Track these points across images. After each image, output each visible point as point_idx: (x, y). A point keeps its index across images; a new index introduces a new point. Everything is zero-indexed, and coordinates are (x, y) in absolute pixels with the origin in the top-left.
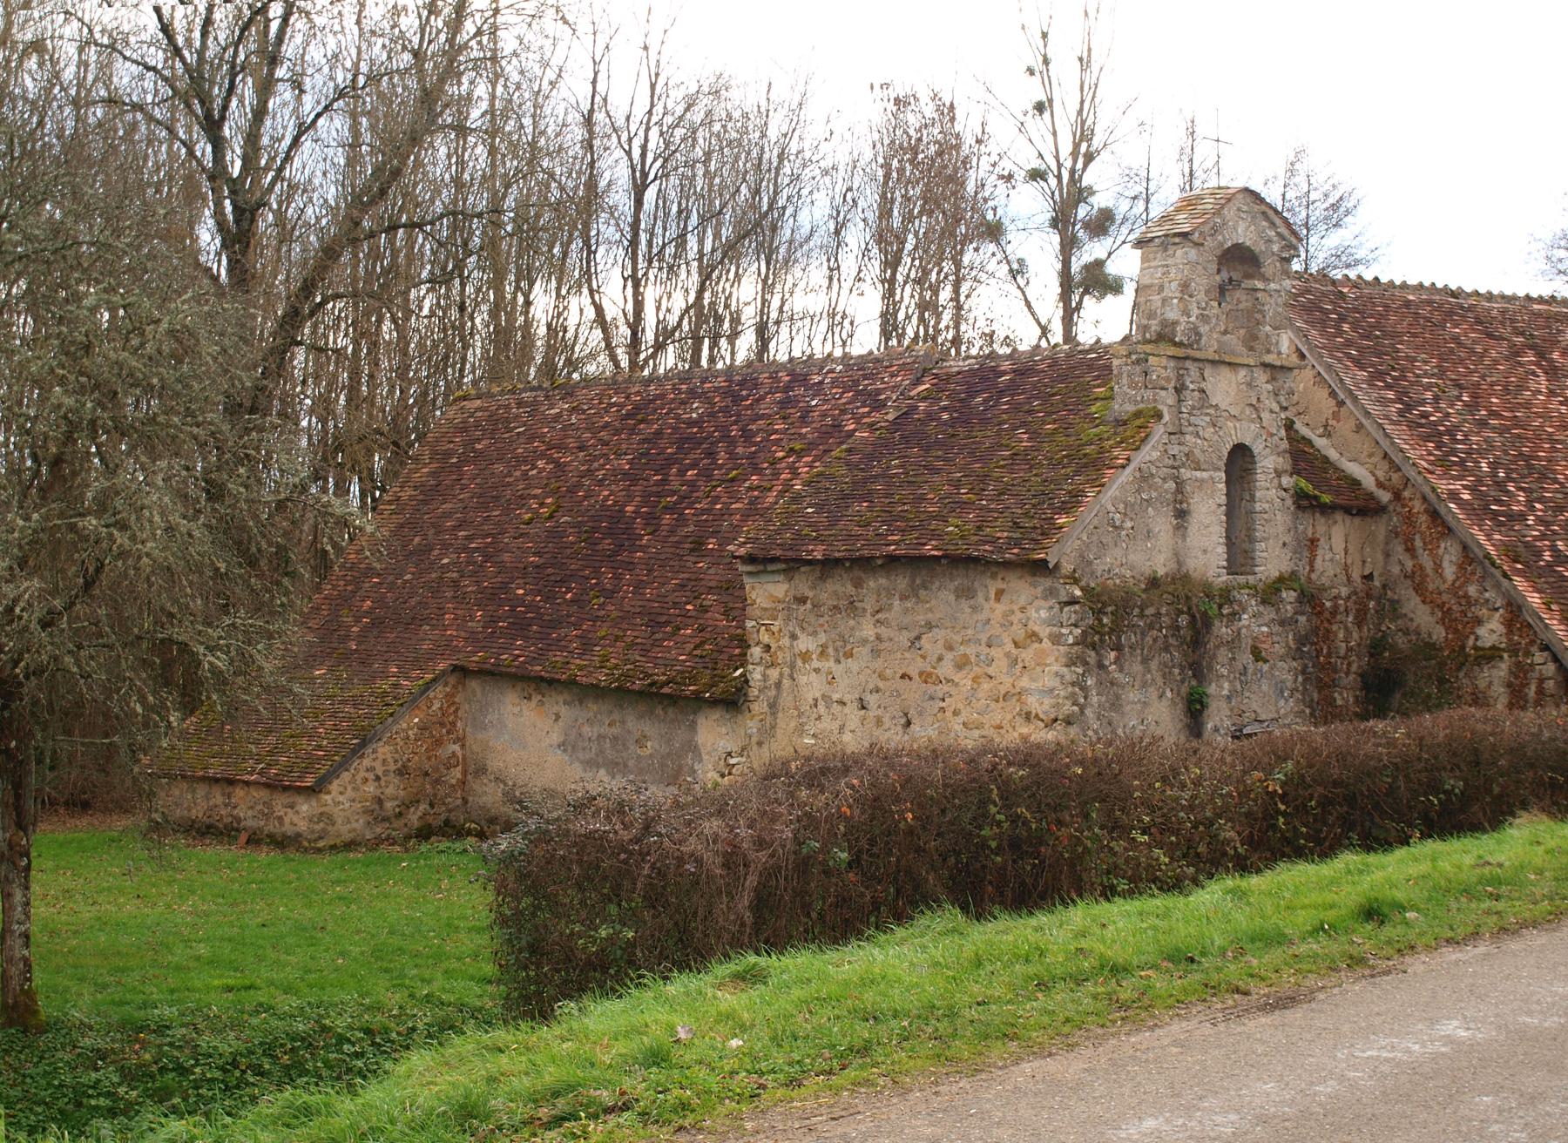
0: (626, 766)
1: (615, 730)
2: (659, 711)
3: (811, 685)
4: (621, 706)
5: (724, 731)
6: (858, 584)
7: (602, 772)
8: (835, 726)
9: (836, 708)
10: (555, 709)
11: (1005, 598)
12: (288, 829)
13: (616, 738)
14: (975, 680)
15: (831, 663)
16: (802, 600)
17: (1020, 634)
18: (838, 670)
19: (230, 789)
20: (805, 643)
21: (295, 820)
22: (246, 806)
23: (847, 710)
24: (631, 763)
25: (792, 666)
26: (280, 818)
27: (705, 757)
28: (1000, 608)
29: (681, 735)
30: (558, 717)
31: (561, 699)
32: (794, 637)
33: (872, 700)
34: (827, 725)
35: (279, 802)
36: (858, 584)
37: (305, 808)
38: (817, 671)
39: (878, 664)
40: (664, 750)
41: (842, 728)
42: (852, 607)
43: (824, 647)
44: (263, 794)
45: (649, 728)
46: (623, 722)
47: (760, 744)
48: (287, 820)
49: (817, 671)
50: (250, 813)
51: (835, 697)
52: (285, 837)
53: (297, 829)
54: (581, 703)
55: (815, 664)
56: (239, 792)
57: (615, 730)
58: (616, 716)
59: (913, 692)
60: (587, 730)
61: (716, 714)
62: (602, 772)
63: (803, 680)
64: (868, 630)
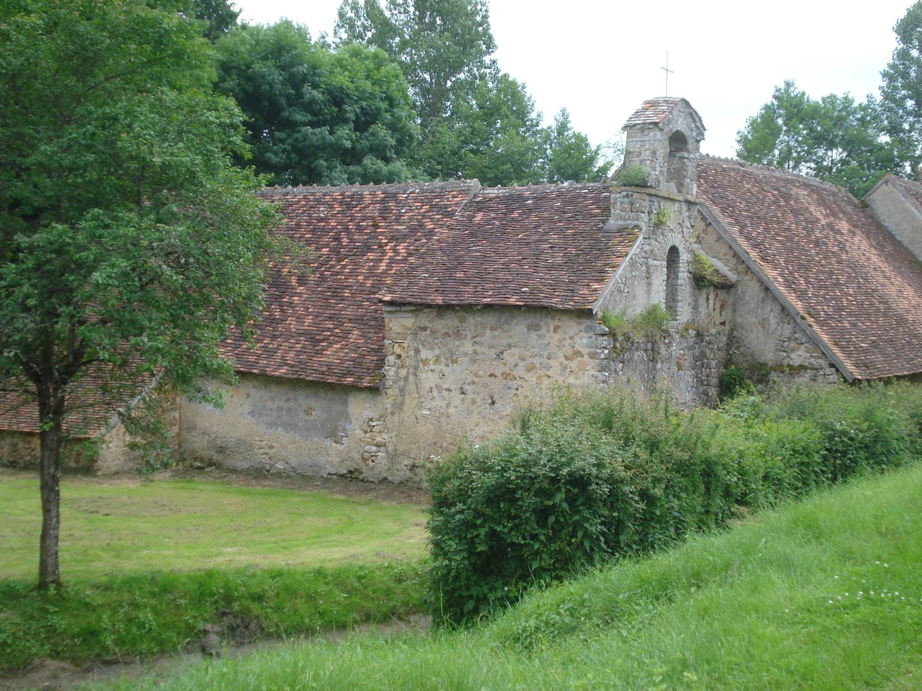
0: (297, 426)
3: (428, 379)
5: (368, 405)
6: (462, 320)
7: (280, 429)
8: (444, 403)
9: (445, 393)
10: (247, 391)
11: (560, 331)
13: (290, 409)
15: (443, 367)
16: (424, 329)
17: (569, 352)
19: (29, 439)
23: (452, 394)
25: (416, 368)
27: (354, 421)
28: (557, 337)
29: (338, 407)
30: (248, 396)
33: (466, 387)
34: (439, 403)
36: (462, 320)
38: (433, 371)
39: (474, 368)
41: (448, 405)
46: (295, 399)
47: (393, 414)
49: (433, 371)
51: (445, 386)
55: (432, 367)
58: (291, 395)
59: (497, 385)
60: (269, 404)
62: (280, 429)
64: (468, 347)
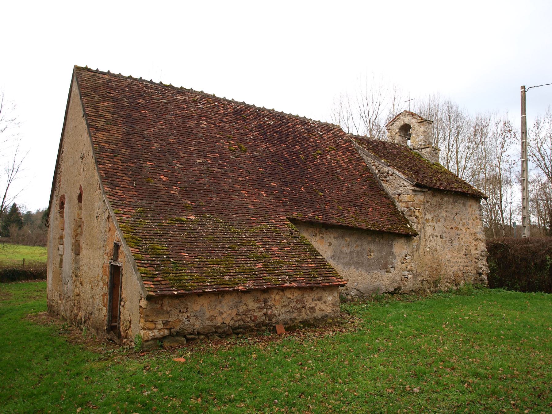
0: (363, 263)
1: (358, 249)
2: (377, 240)
3: (429, 230)
4: (361, 239)
5: (405, 247)
6: (442, 199)
7: (352, 267)
8: (434, 244)
9: (435, 238)
10: (329, 240)
11: (472, 207)
12: (318, 314)
13: (358, 252)
14: (466, 229)
15: (435, 224)
16: (428, 202)
17: (474, 218)
18: (436, 225)
19: (266, 296)
20: (428, 216)
21: (323, 307)
22: (280, 307)
23: (438, 239)
24: (365, 262)
25: (424, 224)
26: (312, 309)
27: (397, 257)
28: (471, 210)
29: (386, 250)
30: (330, 244)
31: (332, 236)
32: (425, 214)
33: (444, 235)
34: (433, 244)
35: (309, 300)
36: (442, 199)
37: (330, 298)
38: (430, 226)
39: (445, 224)
40: (379, 255)
41: (436, 244)
42: (439, 205)
43: (433, 218)
44: (297, 295)
45: (372, 247)
46: (361, 245)
47: (416, 251)
48: (317, 308)
49: (430, 226)
50: (283, 310)
51: (435, 234)
52: (316, 319)
53: (325, 313)
54: (342, 237)
55: (430, 224)
56: (275, 297)
57: (358, 249)
58: (358, 243)
59: (453, 232)
60: (346, 250)
61: (402, 241)
62: (352, 267)
63: (427, 228)
64: (444, 214)
